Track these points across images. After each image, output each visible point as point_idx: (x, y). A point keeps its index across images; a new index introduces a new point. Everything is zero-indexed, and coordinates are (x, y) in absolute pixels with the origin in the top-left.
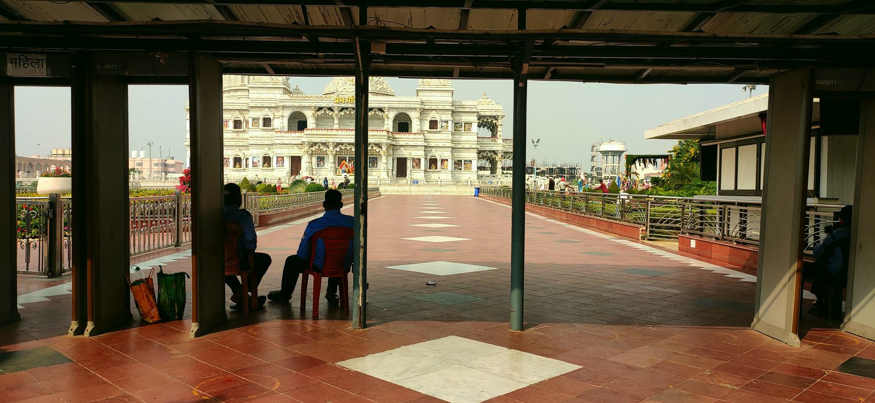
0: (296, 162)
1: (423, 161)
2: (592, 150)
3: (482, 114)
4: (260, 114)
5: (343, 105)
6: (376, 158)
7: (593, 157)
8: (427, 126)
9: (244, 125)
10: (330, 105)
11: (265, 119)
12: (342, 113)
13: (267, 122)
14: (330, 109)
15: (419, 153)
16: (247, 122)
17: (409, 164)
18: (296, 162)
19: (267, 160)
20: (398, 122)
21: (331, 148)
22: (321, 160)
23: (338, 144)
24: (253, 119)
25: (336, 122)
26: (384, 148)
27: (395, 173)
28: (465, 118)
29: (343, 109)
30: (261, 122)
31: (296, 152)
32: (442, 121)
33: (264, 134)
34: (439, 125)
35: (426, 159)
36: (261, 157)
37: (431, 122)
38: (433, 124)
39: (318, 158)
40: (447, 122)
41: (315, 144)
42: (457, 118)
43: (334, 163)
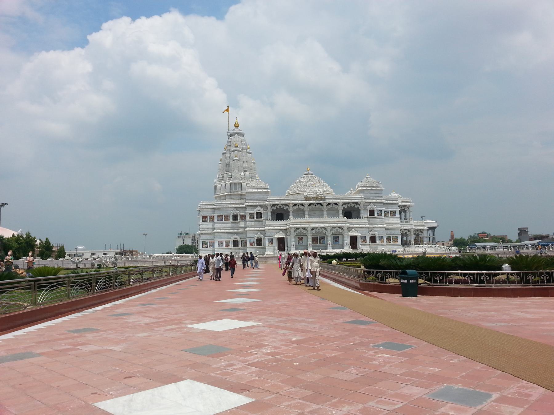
3: (400, 204)
4: (255, 211)
6: (338, 237)
8: (367, 214)
12: (310, 207)
13: (259, 215)
14: (302, 205)
17: (359, 241)
19: (259, 242)
24: (250, 214)
29: (310, 204)
30: (255, 216)
31: (282, 235)
32: (378, 210)
34: (376, 214)
38: (372, 213)
40: (381, 211)
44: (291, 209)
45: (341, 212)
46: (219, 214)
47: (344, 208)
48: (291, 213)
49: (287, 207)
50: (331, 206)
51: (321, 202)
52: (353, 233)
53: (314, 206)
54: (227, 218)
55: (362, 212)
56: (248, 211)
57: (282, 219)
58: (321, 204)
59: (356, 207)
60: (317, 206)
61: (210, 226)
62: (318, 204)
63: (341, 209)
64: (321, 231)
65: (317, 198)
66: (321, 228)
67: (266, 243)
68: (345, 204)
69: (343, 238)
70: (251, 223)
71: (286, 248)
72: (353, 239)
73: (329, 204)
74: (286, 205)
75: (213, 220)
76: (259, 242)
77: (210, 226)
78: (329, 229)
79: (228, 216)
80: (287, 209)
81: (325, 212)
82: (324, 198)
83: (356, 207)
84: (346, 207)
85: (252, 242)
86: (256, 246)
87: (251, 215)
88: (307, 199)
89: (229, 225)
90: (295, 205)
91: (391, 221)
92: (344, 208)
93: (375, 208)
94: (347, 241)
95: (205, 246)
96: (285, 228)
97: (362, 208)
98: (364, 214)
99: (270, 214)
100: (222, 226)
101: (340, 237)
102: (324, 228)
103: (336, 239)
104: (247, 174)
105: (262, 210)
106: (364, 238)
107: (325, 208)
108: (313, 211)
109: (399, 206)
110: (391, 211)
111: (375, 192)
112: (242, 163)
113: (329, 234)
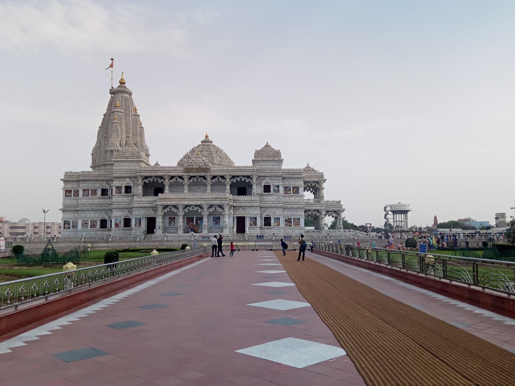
1: (258, 219)
2: (385, 210)
4: (123, 184)
5: (191, 174)
6: (219, 218)
7: (386, 215)
8: (261, 190)
10: (180, 174)
12: (191, 181)
13: (128, 189)
14: (181, 177)
15: (255, 212)
19: (127, 222)
21: (181, 209)
22: (172, 219)
23: (187, 206)
24: (117, 187)
25: (186, 187)
26: (227, 209)
27: (235, 230)
28: (292, 184)
29: (191, 177)
30: (123, 190)
31: (151, 214)
33: (125, 199)
34: (272, 190)
35: (261, 217)
36: (122, 218)
38: (267, 189)
39: (170, 218)
40: (278, 186)
41: (167, 206)
42: (286, 184)
43: (183, 222)
44: (167, 182)
45: (228, 187)
46: (85, 188)
47: (232, 182)
48: (167, 188)
50: (216, 179)
51: (203, 174)
52: (241, 213)
53: (195, 180)
55: (254, 187)
56: (116, 183)
58: (204, 178)
59: (247, 181)
62: (200, 177)
63: (228, 182)
64: (195, 209)
65: (198, 170)
66: (196, 206)
67: (133, 223)
68: (233, 177)
70: (118, 199)
73: (214, 177)
74: (161, 177)
76: (127, 222)
77: (74, 202)
78: (205, 208)
80: (162, 182)
81: (209, 187)
82: (207, 170)
83: (247, 181)
84: (235, 181)
86: (122, 227)
87: (119, 188)
89: (97, 201)
90: (172, 177)
92: (232, 182)
93: (273, 183)
95: (67, 226)
98: (257, 189)
99: (140, 188)
102: (200, 206)
106: (253, 220)
108: (196, 185)
109: (305, 183)
110: (293, 188)
111: (272, 163)
113: (205, 213)
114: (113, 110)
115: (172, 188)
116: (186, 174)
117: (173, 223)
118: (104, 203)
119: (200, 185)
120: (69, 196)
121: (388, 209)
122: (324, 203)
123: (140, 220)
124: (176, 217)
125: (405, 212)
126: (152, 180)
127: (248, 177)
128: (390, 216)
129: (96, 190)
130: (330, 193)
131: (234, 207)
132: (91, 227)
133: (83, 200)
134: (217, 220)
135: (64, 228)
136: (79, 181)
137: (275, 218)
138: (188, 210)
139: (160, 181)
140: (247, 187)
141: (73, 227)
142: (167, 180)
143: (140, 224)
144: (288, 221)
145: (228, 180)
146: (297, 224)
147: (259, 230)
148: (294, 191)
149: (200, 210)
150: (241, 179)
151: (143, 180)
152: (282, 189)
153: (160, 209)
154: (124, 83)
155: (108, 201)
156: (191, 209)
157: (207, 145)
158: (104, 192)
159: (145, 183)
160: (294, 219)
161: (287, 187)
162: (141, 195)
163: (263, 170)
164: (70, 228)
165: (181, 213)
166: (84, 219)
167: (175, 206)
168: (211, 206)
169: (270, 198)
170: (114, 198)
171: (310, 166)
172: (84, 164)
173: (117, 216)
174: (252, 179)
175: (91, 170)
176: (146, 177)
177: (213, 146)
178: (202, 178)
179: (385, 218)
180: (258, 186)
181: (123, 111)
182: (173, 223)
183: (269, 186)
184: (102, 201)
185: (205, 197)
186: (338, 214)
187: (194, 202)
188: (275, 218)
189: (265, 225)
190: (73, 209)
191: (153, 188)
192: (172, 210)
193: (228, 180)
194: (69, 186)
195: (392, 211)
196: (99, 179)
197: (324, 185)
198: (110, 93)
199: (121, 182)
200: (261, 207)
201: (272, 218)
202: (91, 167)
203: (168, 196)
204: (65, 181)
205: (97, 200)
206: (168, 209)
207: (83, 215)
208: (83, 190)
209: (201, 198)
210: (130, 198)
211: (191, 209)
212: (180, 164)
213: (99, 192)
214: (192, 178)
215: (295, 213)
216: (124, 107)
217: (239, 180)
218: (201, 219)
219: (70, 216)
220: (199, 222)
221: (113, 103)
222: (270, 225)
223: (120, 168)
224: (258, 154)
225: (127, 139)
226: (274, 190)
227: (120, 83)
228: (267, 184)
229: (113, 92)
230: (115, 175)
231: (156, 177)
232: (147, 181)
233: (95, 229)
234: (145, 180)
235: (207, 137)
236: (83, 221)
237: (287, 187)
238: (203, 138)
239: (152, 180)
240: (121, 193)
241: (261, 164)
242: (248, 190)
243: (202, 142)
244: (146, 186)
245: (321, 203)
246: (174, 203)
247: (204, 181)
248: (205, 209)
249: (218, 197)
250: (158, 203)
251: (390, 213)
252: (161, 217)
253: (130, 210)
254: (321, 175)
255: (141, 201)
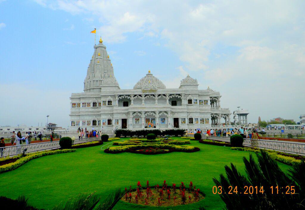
0: (124, 122)
4: (107, 99)
6: (164, 119)
7: (234, 117)
9: (97, 105)
10: (140, 94)
11: (109, 102)
12: (146, 97)
13: (110, 102)
14: (140, 95)
16: (100, 104)
17: (180, 121)
18: (124, 122)
19: (110, 122)
20: (171, 101)
23: (146, 112)
24: (103, 102)
25: (143, 101)
26: (169, 114)
27: (173, 126)
28: (204, 98)
29: (146, 95)
30: (107, 103)
31: (124, 117)
32: (194, 100)
33: (108, 109)
34: (193, 102)
36: (107, 120)
37: (189, 100)
38: (190, 101)
40: (196, 100)
42: (200, 99)
44: (132, 98)
45: (168, 101)
47: (170, 98)
48: (132, 101)
49: (130, 97)
51: (153, 94)
52: (176, 116)
54: (89, 104)
55: (183, 101)
56: (103, 99)
57: (127, 105)
58: (154, 95)
60: (151, 97)
61: (77, 110)
62: (151, 95)
63: (168, 98)
64: (151, 114)
66: (152, 112)
68: (171, 95)
69: (168, 119)
70: (104, 108)
71: (127, 126)
72: (176, 121)
73: (159, 95)
74: (129, 96)
75: (80, 106)
76: (110, 122)
77: (77, 110)
79: (90, 103)
81: (157, 101)
82: (155, 91)
83: (179, 97)
84: (171, 97)
85: (104, 122)
88: (144, 91)
90: (135, 95)
91: (204, 107)
92: (170, 98)
93: (193, 98)
94: (171, 122)
96: (126, 112)
97: (182, 98)
98: (185, 102)
99: (117, 102)
100: (85, 111)
101: (166, 119)
102: (154, 112)
103: (163, 120)
104: (106, 75)
105: (111, 99)
106: (184, 120)
107: (156, 97)
112: (103, 67)
113: (157, 116)
114: (96, 58)
115: (134, 102)
116: (143, 93)
117: (138, 122)
118: (94, 111)
119: (151, 100)
120: (74, 107)
121: (236, 113)
122: (220, 109)
123: (118, 120)
124: (140, 119)
125: (246, 115)
126: (123, 97)
127: (179, 95)
128: (237, 117)
129: (90, 103)
130: (223, 104)
131: (173, 112)
132: (87, 125)
133: (82, 109)
134: (163, 120)
135: (72, 125)
136: (80, 98)
137: (195, 119)
138: (147, 114)
139: (128, 98)
140: (177, 101)
141: (77, 125)
142: (132, 97)
143: (118, 123)
144: (202, 120)
145: (167, 97)
146: (207, 122)
147: (187, 126)
148: (205, 103)
149: (154, 114)
150: (175, 96)
151: (118, 97)
152: (198, 101)
153: (131, 114)
154: (102, 42)
155: (97, 110)
156: (149, 114)
157: (150, 77)
158: (94, 104)
159: (119, 99)
160: (205, 119)
161: (201, 101)
162: (118, 106)
163: (187, 91)
164: (75, 125)
165: (143, 116)
166: (83, 120)
167: (140, 112)
168: (160, 112)
169: (193, 107)
170: (102, 108)
171: (210, 88)
172: (80, 90)
173: (104, 118)
174: (181, 96)
175: (84, 92)
176: (120, 96)
177: (154, 77)
178: (152, 96)
179: (234, 118)
180: (185, 100)
181: (102, 58)
182: (138, 122)
183: (191, 100)
184: (93, 110)
185: (157, 106)
186: (227, 116)
187: (151, 110)
188: (195, 119)
189: (190, 123)
190: (77, 114)
191: (123, 102)
192: (138, 114)
193: (167, 97)
194: (74, 102)
195: (238, 114)
196: (91, 97)
197: (220, 99)
198: (94, 48)
199: (105, 99)
200: (187, 112)
201: (193, 118)
202: (84, 90)
203: (133, 106)
204: (71, 99)
205: (91, 109)
206: (136, 114)
207: (83, 118)
208: (83, 103)
209: (155, 108)
210: (111, 108)
211: (149, 114)
212: (135, 88)
213: (92, 105)
214: (147, 96)
215: (206, 116)
216: (102, 55)
217: (174, 96)
218: (154, 119)
219: (75, 119)
220: (153, 121)
221: (97, 53)
222: (192, 123)
223: (105, 91)
224: (184, 81)
225: (105, 74)
226: (194, 102)
227: (100, 42)
228: (190, 99)
229: (96, 48)
230: (102, 95)
231: (126, 95)
232: (121, 98)
233: (90, 126)
234: (119, 97)
235: (149, 72)
236: (83, 121)
237: (201, 101)
238: (147, 73)
239: (123, 97)
240: (106, 105)
241: (186, 87)
242: (178, 103)
243: (147, 75)
244: (119, 101)
245: (219, 109)
246: (139, 110)
247: (154, 97)
248: (157, 114)
249: (165, 106)
250: (130, 110)
251: (237, 115)
252: (131, 119)
253: (112, 114)
254: (219, 93)
255: (118, 109)
